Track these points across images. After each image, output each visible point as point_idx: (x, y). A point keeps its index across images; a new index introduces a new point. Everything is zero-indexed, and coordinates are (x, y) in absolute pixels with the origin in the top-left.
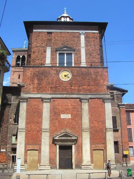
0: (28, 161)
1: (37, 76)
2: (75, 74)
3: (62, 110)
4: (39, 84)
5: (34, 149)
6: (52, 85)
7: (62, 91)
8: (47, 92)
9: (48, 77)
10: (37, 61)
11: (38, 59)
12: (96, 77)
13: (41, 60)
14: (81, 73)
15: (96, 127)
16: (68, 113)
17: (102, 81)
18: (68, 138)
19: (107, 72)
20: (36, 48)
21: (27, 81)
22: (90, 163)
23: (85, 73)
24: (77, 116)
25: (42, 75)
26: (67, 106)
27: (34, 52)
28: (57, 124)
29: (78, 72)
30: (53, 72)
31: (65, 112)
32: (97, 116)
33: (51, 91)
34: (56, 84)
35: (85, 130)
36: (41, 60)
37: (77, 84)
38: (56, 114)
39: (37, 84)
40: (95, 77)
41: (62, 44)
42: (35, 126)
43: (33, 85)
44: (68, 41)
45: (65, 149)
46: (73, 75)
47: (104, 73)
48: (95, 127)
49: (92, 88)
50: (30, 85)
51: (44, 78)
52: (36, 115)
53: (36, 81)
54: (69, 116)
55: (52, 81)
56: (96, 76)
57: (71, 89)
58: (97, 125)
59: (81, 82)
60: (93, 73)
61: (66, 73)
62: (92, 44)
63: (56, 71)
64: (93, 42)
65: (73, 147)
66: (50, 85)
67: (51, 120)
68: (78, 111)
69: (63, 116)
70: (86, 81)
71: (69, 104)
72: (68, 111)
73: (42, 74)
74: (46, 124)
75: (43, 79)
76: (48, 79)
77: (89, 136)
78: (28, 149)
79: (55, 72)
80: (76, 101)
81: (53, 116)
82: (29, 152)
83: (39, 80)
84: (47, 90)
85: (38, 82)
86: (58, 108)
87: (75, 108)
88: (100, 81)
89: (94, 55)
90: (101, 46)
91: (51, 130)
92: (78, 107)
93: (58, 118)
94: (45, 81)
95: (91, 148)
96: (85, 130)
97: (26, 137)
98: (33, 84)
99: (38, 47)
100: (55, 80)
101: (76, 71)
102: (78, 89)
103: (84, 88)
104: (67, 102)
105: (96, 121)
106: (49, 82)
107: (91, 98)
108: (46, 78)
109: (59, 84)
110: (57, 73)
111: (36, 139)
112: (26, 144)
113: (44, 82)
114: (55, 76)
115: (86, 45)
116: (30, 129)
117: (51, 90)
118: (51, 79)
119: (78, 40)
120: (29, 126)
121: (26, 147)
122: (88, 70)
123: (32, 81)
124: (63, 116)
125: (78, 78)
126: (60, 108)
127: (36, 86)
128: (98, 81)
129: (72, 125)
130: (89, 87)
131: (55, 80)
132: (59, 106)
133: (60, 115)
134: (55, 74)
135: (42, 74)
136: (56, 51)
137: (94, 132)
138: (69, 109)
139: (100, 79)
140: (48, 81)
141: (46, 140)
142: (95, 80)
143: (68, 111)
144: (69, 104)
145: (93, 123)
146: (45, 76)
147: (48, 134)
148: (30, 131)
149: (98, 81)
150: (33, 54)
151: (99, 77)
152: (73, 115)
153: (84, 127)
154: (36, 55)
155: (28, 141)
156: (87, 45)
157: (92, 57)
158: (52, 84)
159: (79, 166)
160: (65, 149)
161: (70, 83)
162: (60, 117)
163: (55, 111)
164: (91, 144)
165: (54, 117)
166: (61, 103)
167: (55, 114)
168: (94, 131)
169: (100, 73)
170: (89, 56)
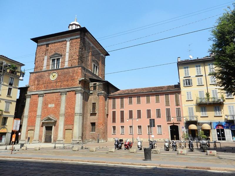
5: (32, 129)
8: (42, 89)
16: (53, 103)
17: (76, 77)
24: (58, 105)
25: (40, 77)
26: (53, 98)
28: (46, 111)
29: (62, 72)
30: (46, 74)
32: (71, 105)
41: (55, 52)
44: (58, 49)
45: (49, 128)
46: (58, 75)
54: (53, 105)
56: (73, 74)
58: (70, 111)
61: (54, 74)
62: (74, 48)
65: (53, 127)
67: (43, 109)
68: (59, 101)
69: (50, 106)
71: (54, 97)
72: (53, 102)
74: (39, 112)
79: (48, 74)
80: (59, 94)
81: (44, 106)
83: (38, 81)
87: (58, 99)
92: (59, 98)
93: (47, 107)
95: (64, 128)
97: (28, 121)
101: (60, 72)
107: (68, 91)
112: (28, 126)
118: (45, 80)
119: (65, 47)
121: (27, 128)
122: (68, 70)
129: (55, 112)
133: (48, 105)
136: (50, 58)
141: (38, 122)
143: (53, 102)
144: (54, 97)
147: (39, 119)
148: (30, 117)
155: (29, 124)
160: (49, 128)
161: (56, 81)
165: (45, 107)
167: (45, 104)
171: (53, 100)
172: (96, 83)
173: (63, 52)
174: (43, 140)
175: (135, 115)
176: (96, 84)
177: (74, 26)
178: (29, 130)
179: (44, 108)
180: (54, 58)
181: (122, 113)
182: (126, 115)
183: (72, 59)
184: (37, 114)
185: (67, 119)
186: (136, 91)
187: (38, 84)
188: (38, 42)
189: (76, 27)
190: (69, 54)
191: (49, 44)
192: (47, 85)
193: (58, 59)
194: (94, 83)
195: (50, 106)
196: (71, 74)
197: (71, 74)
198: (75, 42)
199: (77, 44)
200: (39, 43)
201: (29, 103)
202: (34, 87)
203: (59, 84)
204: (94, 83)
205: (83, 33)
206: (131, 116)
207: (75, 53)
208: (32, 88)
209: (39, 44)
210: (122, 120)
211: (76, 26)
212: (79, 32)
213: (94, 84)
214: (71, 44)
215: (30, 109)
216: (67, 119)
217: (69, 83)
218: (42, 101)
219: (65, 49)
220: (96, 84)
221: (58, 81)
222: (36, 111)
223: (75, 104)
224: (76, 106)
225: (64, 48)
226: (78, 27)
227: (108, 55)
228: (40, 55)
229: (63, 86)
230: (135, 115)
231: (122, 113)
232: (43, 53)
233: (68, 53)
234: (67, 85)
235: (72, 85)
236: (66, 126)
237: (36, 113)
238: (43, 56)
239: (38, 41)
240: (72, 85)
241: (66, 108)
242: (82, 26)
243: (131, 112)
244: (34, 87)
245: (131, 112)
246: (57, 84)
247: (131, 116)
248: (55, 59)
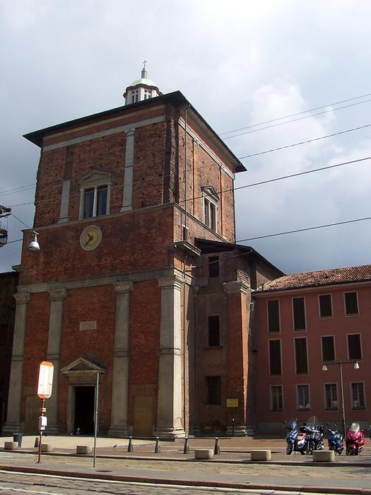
0: (27, 416)
16: (92, 319)
17: (160, 239)
23: (127, 225)
31: (87, 317)
51: (54, 249)
57: (98, 266)
60: (142, 224)
62: (149, 152)
64: (152, 148)
68: (110, 313)
69: (83, 326)
70: (128, 244)
77: (125, 367)
86: (76, 310)
93: (74, 331)
98: (36, 265)
101: (110, 226)
103: (122, 261)
115: (137, 158)
116: (30, 356)
124: (83, 326)
131: (72, 252)
133: (78, 324)
148: (30, 359)
151: (154, 230)
156: (138, 158)
158: (67, 260)
161: (99, 253)
167: (70, 321)
172: (216, 254)
173: (117, 167)
174: (70, 424)
175: (341, 348)
176: (217, 258)
177: (142, 90)
180: (91, 187)
181: (301, 344)
182: (314, 350)
183: (145, 184)
184: (49, 352)
186: (339, 277)
187: (47, 263)
188: (44, 144)
189: (148, 94)
190: (135, 171)
193: (102, 189)
194: (212, 255)
196: (143, 229)
197: (143, 229)
198: (151, 136)
199: (155, 142)
200: (46, 145)
201: (24, 317)
202: (35, 272)
203: (106, 260)
204: (212, 255)
205: (173, 110)
206: (329, 355)
207: (151, 168)
208: (31, 277)
209: (46, 149)
210: (302, 367)
211: (146, 91)
212: (162, 107)
213: (211, 259)
214: (139, 143)
215: (27, 335)
218: (60, 314)
219: (123, 158)
220: (217, 258)
222: (45, 343)
223: (160, 320)
224: (162, 327)
225: (117, 153)
226: (155, 94)
227: (239, 168)
228: (51, 179)
230: (341, 348)
231: (301, 344)
232: (58, 172)
233: (131, 169)
237: (43, 347)
238: (59, 182)
239: (44, 138)
241: (131, 333)
242: (165, 91)
243: (328, 342)
244: (35, 272)
245: (328, 342)
246: (100, 261)
247: (329, 355)
248: (93, 189)
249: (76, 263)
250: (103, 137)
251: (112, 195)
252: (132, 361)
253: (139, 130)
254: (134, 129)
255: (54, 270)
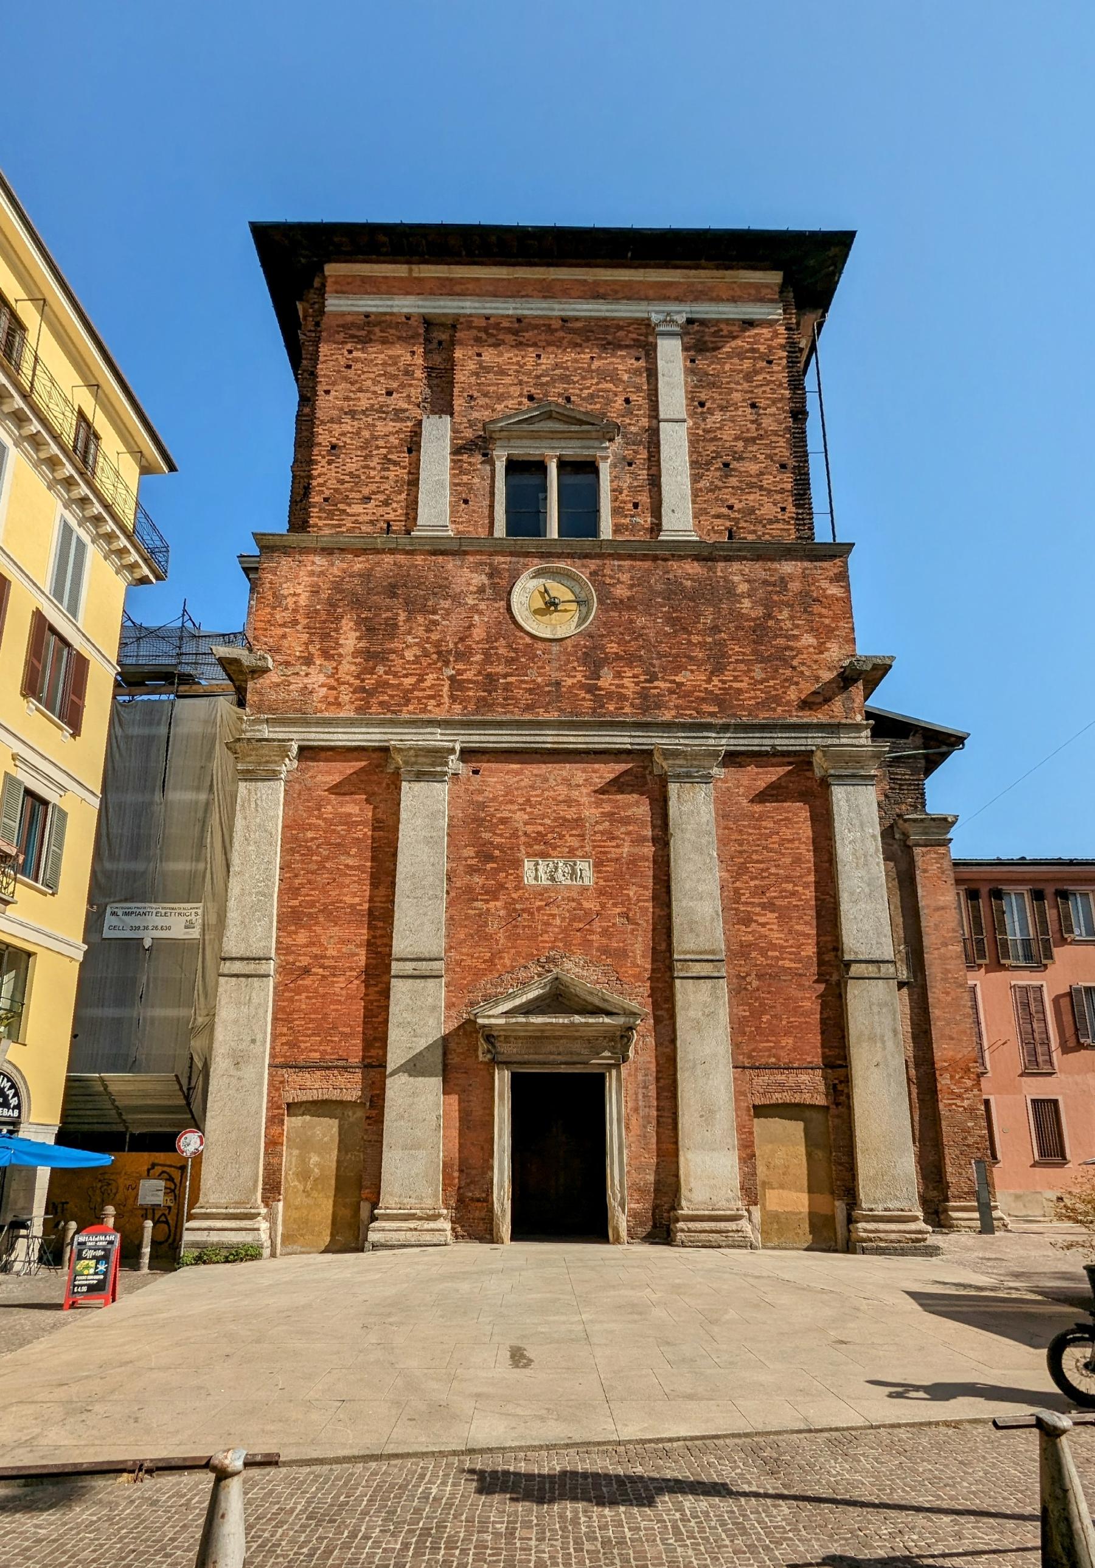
1: (357, 603)
2: (621, 592)
3: (529, 829)
4: (371, 657)
6: (460, 666)
7: (529, 708)
8: (424, 710)
9: (434, 613)
10: (357, 509)
11: (366, 491)
12: (769, 616)
13: (386, 503)
14: (659, 587)
15: (773, 946)
18: (578, 1019)
19: (842, 577)
20: (347, 419)
21: (284, 636)
22: (738, 1205)
23: (689, 583)
25: (393, 595)
26: (569, 802)
27: (334, 447)
30: (467, 577)
33: (457, 708)
34: (488, 658)
35: (697, 969)
36: (386, 503)
37: (630, 659)
38: (490, 858)
39: (356, 653)
40: (760, 612)
41: (531, 398)
42: (343, 942)
43: (330, 665)
47: (824, 584)
48: (763, 953)
49: (736, 685)
50: (308, 661)
51: (403, 616)
52: (350, 862)
53: (349, 639)
55: (462, 639)
57: (591, 689)
59: (664, 648)
62: (737, 396)
63: (491, 576)
64: (746, 385)
66: (447, 663)
67: (460, 897)
70: (695, 639)
72: (574, 842)
73: (392, 591)
74: (420, 924)
75: (396, 626)
76: (435, 623)
78: (291, 1095)
79: (484, 579)
81: (472, 870)
82: (291, 1123)
83: (368, 629)
84: (430, 697)
85: (362, 644)
86: (504, 821)
87: (626, 821)
88: (796, 638)
89: (753, 468)
90: (799, 414)
91: (459, 963)
93: (502, 886)
94: (410, 639)
95: (739, 1094)
96: (697, 969)
98: (326, 655)
99: (363, 412)
100: (478, 633)
102: (644, 695)
103: (680, 685)
104: (567, 782)
105: (770, 906)
106: (437, 644)
108: (420, 619)
109: (510, 661)
110: (494, 586)
111: (347, 1030)
113: (409, 645)
114: (482, 606)
115: (698, 406)
116: (304, 961)
117: (453, 698)
118: (452, 625)
120: (302, 938)
123: (325, 636)
125: (641, 621)
126: (520, 817)
127: (348, 668)
128: (781, 641)
130: (716, 681)
131: (478, 633)
132: (512, 802)
134: (481, 590)
135: (392, 591)
137: (755, 984)
138: (579, 822)
139: (797, 626)
140: (435, 636)
142: (760, 632)
145: (747, 921)
146: (414, 607)
147: (436, 993)
148: (306, 971)
149: (781, 641)
150: (329, 463)
152: (610, 868)
153: (686, 947)
154: (351, 467)
156: (702, 404)
157: (733, 481)
158: (461, 656)
159: (661, 1229)
162: (519, 878)
163: (486, 836)
164: (746, 1065)
165: (478, 880)
166: (526, 782)
167: (484, 855)
168: (759, 977)
169: (795, 586)
170: (713, 474)
171: (564, 822)
178: (293, 1108)
179: (469, 890)
185: (756, 1014)
191: (453, 324)
192: (491, 679)
195: (534, 873)
197: (747, 603)
202: (322, 679)
216: (756, 1014)
217: (736, 679)
221: (613, 648)
229: (674, 701)
234: (721, 701)
235: (777, 700)
236: (764, 1079)
240: (777, 700)
241: (736, 913)
244: (322, 679)
249: (500, 669)
250: (564, 320)
251: (617, 491)
252: (738, 992)
253: (696, 327)
254: (681, 319)
255: (411, 680)
